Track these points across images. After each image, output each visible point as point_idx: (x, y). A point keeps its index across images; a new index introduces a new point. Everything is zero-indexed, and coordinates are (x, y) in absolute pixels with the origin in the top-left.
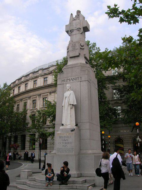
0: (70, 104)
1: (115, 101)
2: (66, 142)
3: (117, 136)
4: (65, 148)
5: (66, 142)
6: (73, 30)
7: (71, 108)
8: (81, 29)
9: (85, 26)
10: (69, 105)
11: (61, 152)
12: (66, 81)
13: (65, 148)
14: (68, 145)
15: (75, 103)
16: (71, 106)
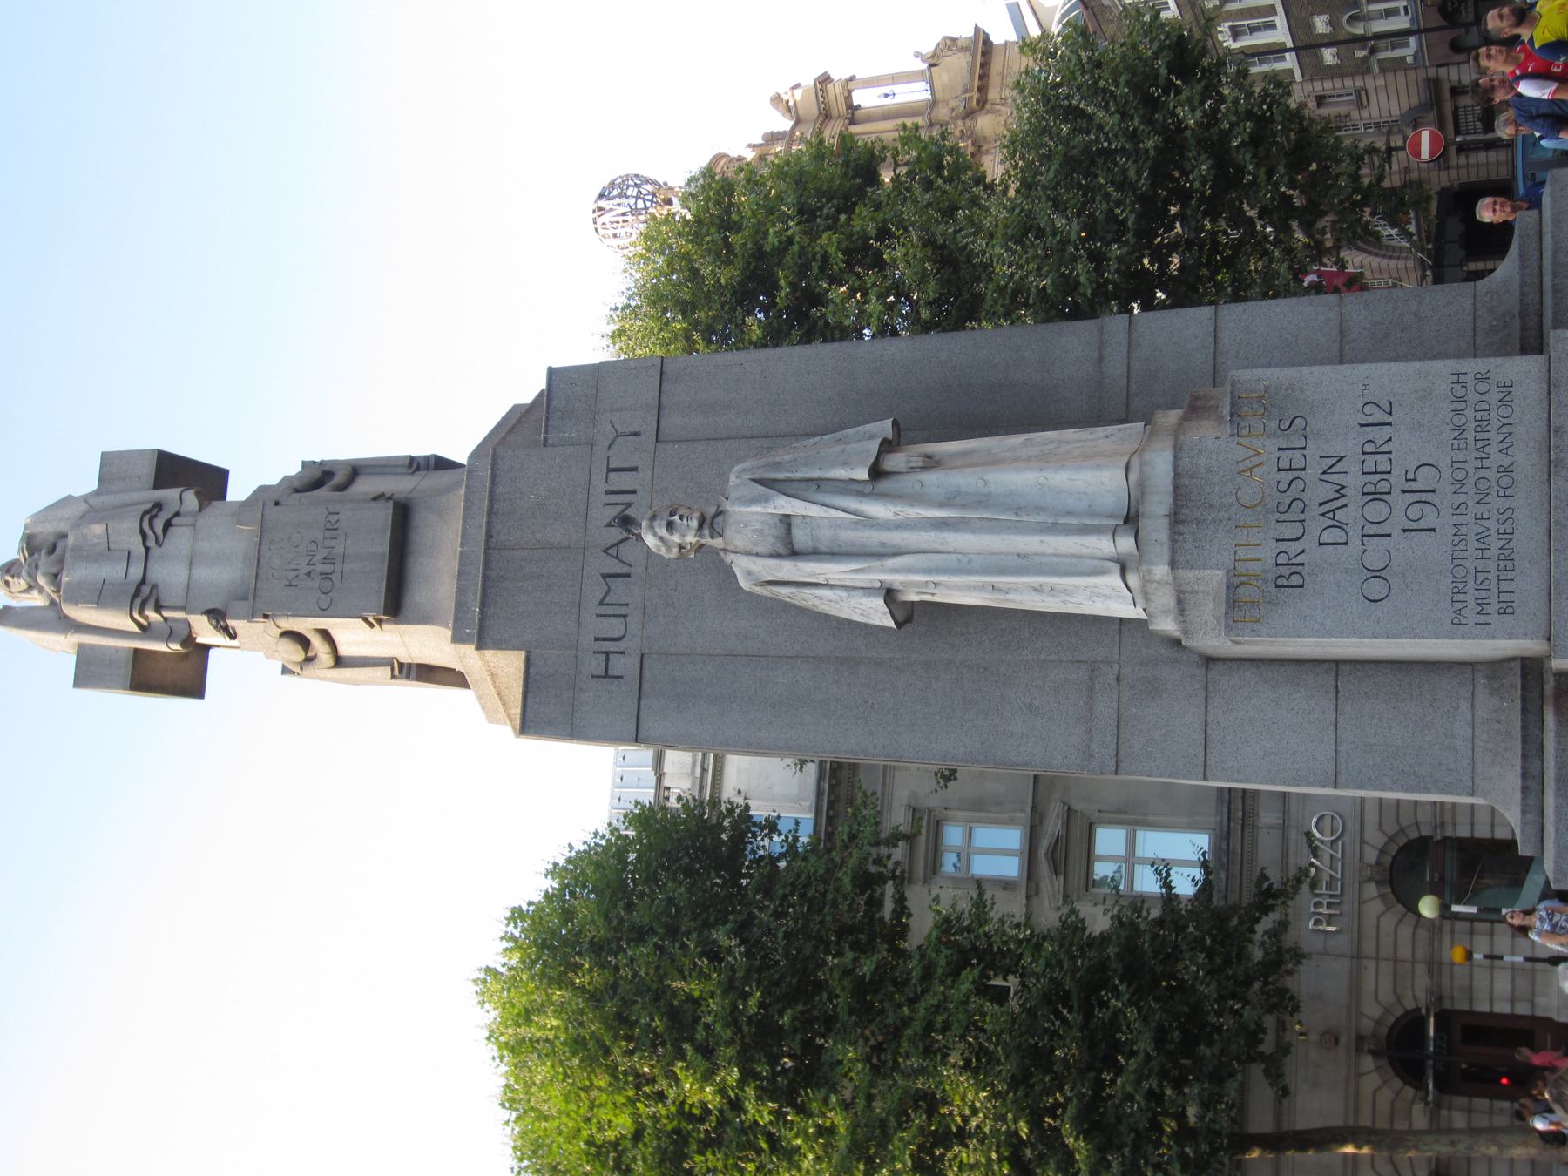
0: (877, 473)
1: (1044, 868)
2: (1354, 481)
3: (1371, 890)
4: (1445, 499)
5: (1354, 481)
6: (146, 590)
7: (931, 463)
8: (158, 506)
9: (148, 470)
10: (885, 485)
11: (1508, 563)
12: (614, 627)
13: (1445, 499)
14: (1408, 448)
15: (885, 428)
16: (894, 461)
